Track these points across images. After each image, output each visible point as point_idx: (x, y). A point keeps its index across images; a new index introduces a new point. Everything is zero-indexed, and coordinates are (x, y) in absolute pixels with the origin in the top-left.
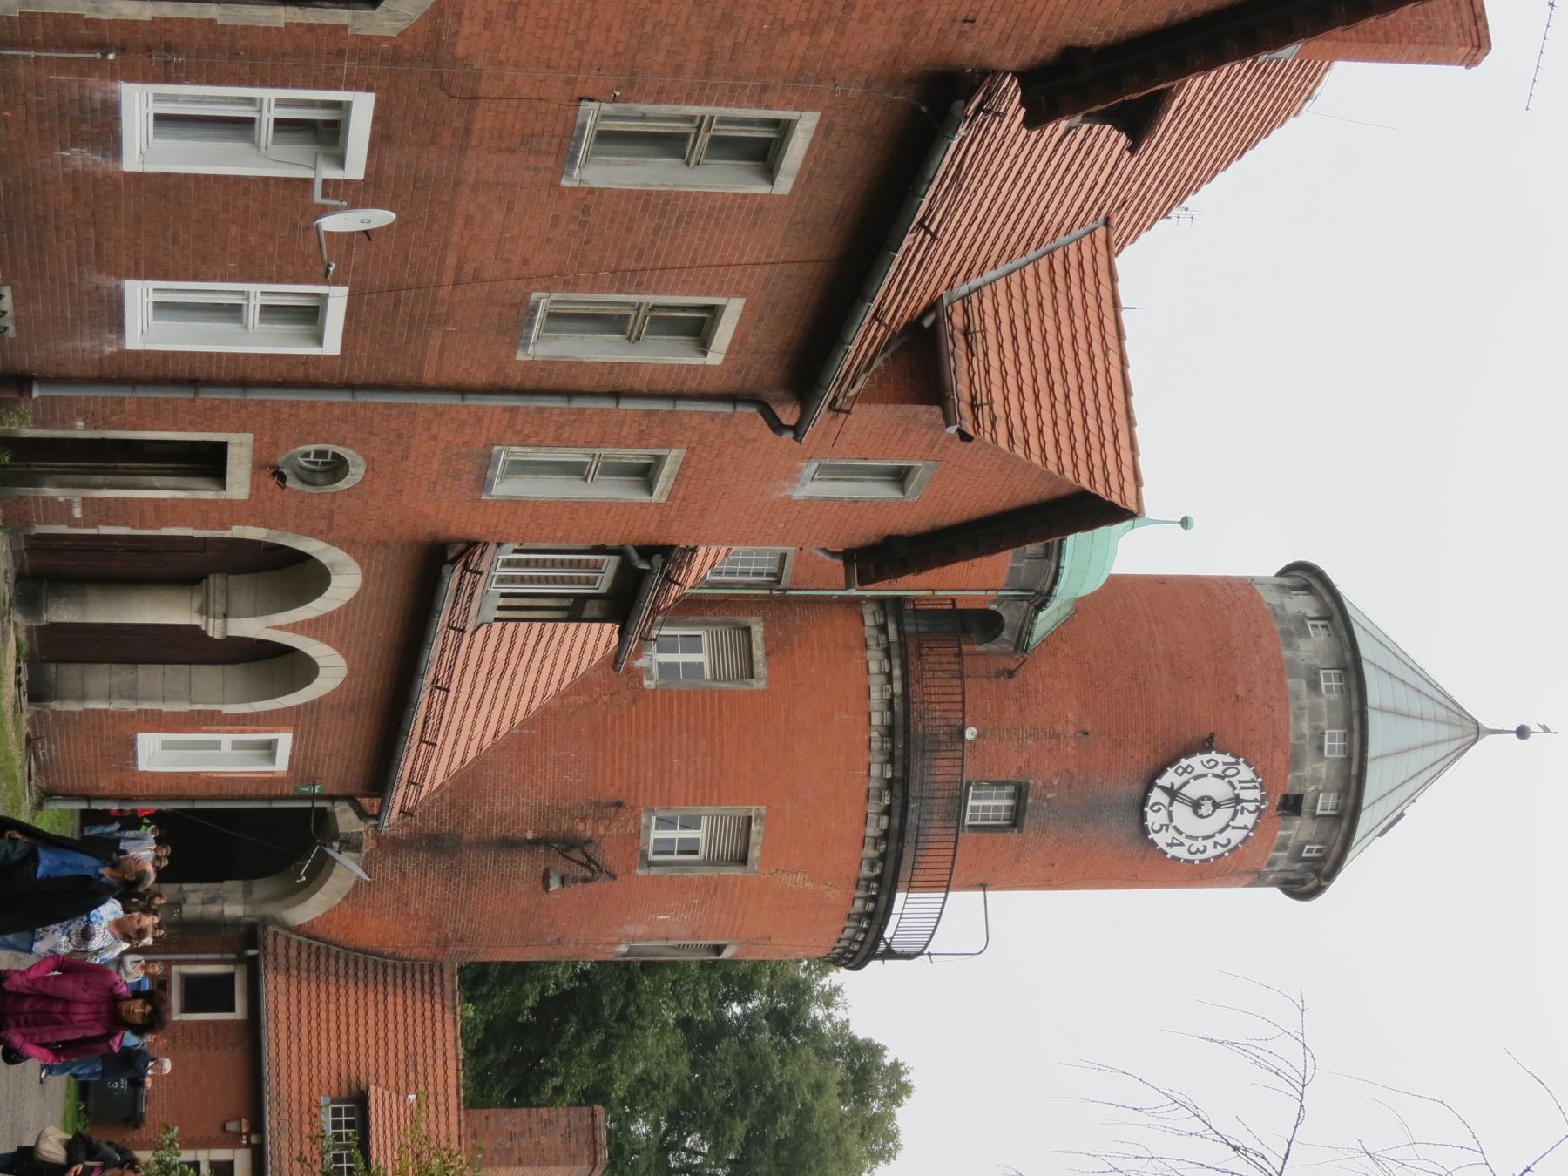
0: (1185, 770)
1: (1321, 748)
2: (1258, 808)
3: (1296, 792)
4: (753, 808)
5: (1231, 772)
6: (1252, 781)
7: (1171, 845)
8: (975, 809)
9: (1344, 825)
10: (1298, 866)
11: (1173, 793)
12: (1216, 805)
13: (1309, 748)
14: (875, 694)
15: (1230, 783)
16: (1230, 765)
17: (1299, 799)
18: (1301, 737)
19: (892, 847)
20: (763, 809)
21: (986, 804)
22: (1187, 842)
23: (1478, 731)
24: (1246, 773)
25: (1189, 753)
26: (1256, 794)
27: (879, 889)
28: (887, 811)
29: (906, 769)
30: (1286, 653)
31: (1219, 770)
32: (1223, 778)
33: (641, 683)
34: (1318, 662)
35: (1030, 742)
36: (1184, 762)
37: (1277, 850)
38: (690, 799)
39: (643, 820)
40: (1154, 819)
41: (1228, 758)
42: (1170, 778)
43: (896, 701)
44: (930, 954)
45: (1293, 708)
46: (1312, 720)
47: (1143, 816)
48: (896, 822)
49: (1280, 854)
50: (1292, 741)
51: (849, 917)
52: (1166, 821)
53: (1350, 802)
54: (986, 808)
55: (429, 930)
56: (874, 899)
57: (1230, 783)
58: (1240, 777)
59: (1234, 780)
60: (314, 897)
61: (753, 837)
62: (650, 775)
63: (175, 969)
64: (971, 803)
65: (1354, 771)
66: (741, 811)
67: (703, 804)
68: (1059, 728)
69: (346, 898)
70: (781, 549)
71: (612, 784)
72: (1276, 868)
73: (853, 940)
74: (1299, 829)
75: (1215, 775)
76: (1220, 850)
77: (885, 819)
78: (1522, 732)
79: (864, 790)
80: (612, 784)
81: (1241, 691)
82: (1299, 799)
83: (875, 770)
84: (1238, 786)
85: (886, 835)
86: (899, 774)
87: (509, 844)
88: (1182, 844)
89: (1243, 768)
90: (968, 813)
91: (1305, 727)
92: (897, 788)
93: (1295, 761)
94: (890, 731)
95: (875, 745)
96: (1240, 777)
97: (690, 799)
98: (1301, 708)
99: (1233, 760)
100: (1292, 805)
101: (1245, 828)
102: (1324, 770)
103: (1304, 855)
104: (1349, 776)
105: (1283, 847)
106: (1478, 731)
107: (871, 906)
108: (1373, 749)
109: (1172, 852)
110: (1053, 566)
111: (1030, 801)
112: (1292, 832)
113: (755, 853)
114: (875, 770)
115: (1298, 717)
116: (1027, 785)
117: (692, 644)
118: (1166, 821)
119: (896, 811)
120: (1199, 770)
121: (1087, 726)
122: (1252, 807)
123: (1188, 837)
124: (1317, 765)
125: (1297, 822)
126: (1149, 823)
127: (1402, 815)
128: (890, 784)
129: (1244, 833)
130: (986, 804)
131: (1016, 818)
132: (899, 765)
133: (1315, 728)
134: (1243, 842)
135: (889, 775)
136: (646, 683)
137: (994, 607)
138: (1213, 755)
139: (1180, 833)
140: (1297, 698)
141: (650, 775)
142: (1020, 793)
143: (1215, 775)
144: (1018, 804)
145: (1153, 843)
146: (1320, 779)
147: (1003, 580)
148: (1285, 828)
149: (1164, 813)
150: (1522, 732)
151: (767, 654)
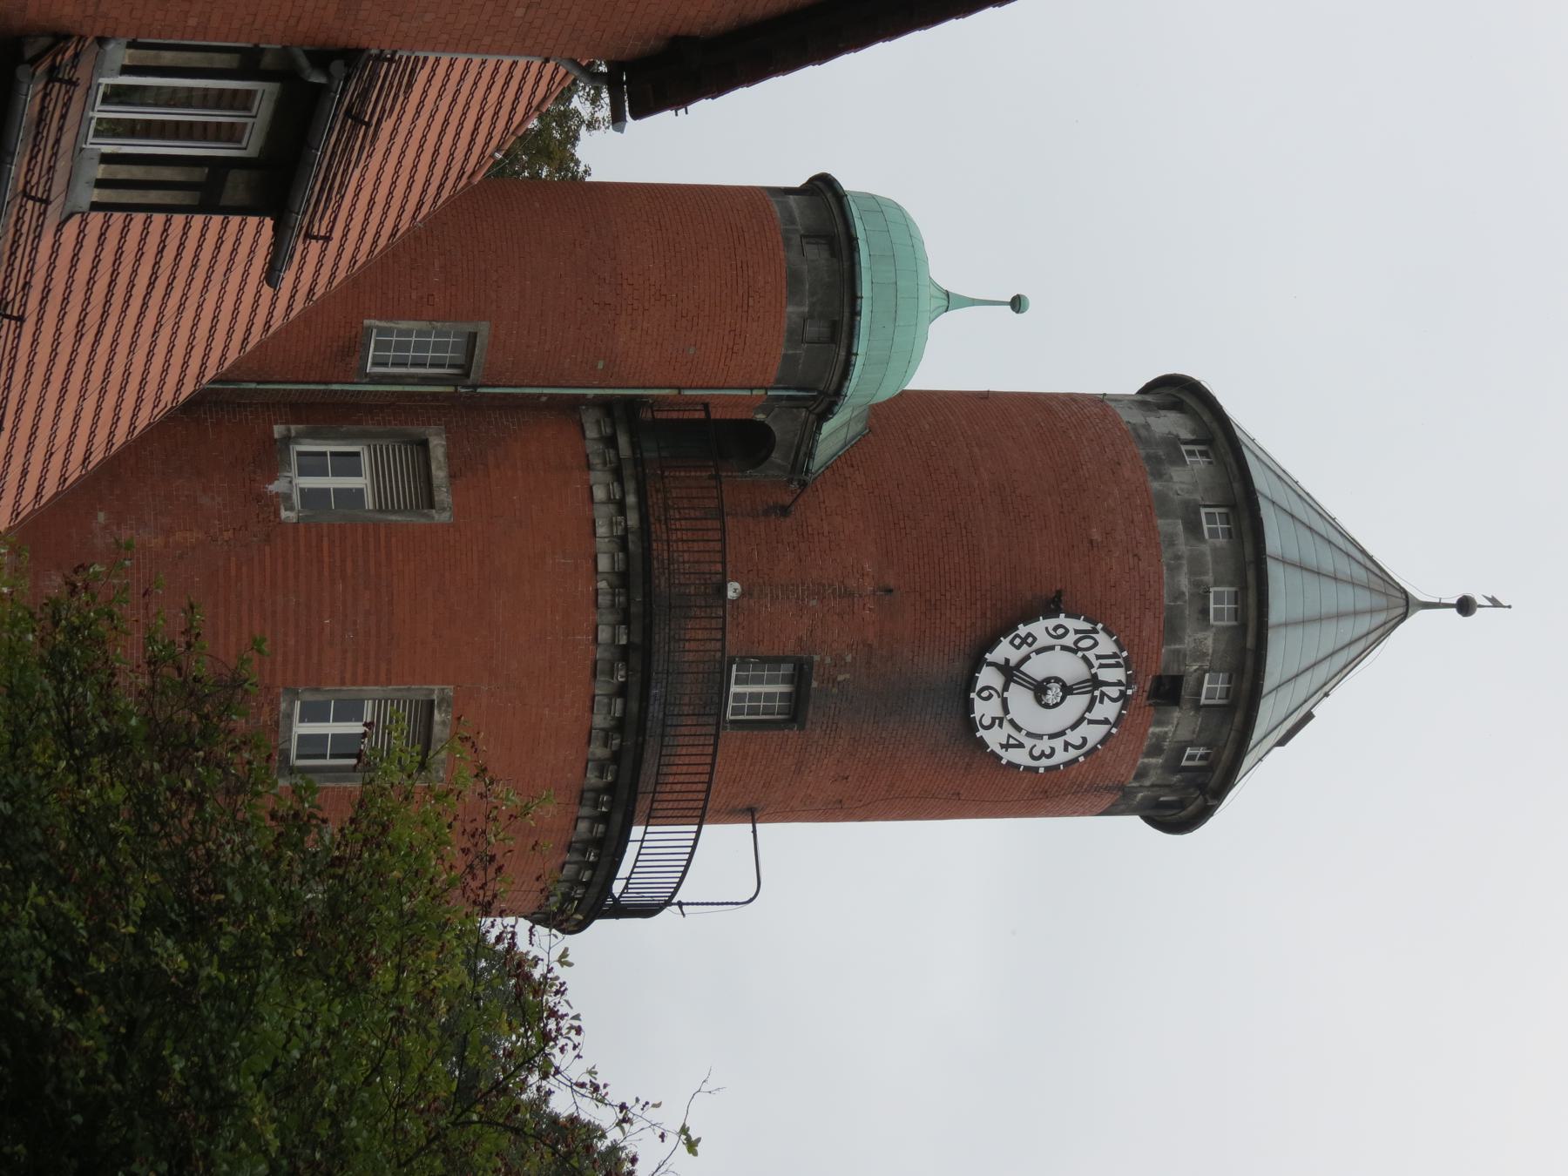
0: (1024, 641)
1: (1205, 612)
2: (1123, 694)
3: (1174, 671)
4: (436, 688)
6: (1114, 656)
7: (1006, 746)
8: (739, 697)
9: (1238, 718)
10: (1176, 778)
11: (1010, 672)
12: (1067, 690)
13: (1189, 611)
14: (602, 530)
15: (1085, 658)
16: (1085, 634)
19: (629, 743)
20: (450, 690)
21: (756, 691)
22: (1028, 742)
23: (1407, 605)
24: (1106, 645)
25: (1029, 618)
26: (1118, 674)
27: (612, 804)
28: (622, 691)
29: (648, 632)
30: (1155, 485)
31: (1069, 640)
32: (1074, 650)
33: (277, 514)
34: (1198, 497)
35: (814, 603)
36: (1022, 630)
37: (1148, 754)
38: (348, 676)
39: (283, 706)
40: (984, 710)
42: (1004, 651)
43: (630, 537)
44: (680, 904)
45: (1166, 556)
46: (1192, 573)
47: (969, 706)
48: (634, 706)
49: (1153, 761)
50: (1166, 601)
51: (569, 847)
52: (1000, 714)
53: (1246, 685)
54: (755, 697)
56: (605, 818)
57: (1085, 658)
58: (1098, 650)
59: (1090, 655)
61: (437, 729)
62: (292, 642)
64: (734, 689)
65: (1250, 642)
66: (418, 692)
67: (365, 683)
68: (852, 583)
70: (468, 327)
72: (1147, 783)
73: (575, 882)
74: (1178, 725)
75: (1064, 648)
76: (1072, 753)
77: (619, 702)
78: (1465, 606)
79: (589, 663)
81: (1096, 535)
83: (604, 634)
84: (1096, 663)
85: (620, 726)
86: (637, 639)
88: (1021, 745)
89: (1101, 637)
90: (731, 703)
91: (1184, 583)
93: (1172, 630)
94: (622, 579)
95: (604, 600)
96: (1098, 650)
97: (348, 676)
98: (1178, 557)
99: (1088, 626)
100: (1168, 691)
101: (1106, 721)
102: (1210, 642)
103: (1184, 763)
104: (1244, 649)
105: (1155, 750)
106: (1407, 605)
107: (601, 828)
108: (1276, 613)
110: (843, 353)
111: (814, 684)
112: (1169, 729)
114: (604, 634)
115: (1174, 570)
116: (811, 662)
117: (347, 464)
118: (1000, 714)
119: (634, 691)
120: (1043, 640)
121: (891, 582)
122: (1114, 692)
123: (1029, 734)
124: (1200, 635)
125: (1176, 714)
126: (977, 715)
127: (1309, 717)
128: (624, 653)
129: (1104, 729)
130: (756, 691)
131: (796, 709)
133: (1196, 584)
134: (1103, 742)
135: (623, 641)
136: (284, 514)
137: (760, 417)
138: (1062, 619)
139: (1019, 729)
140: (1172, 544)
141: (292, 642)
142: (801, 675)
143: (1064, 648)
145: (982, 744)
146: (1205, 654)
147: (773, 373)
148: (1159, 723)
149: (996, 700)
150: (1465, 606)
151: (452, 476)
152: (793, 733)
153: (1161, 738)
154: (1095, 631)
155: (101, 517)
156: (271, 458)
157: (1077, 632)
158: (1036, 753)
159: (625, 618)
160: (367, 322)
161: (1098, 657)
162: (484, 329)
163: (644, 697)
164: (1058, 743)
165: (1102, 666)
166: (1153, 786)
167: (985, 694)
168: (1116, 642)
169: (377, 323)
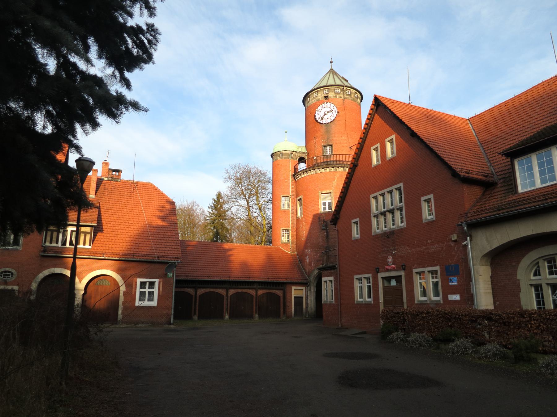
11: (322, 119)
13: (317, 98)
17: (325, 97)
24: (319, 108)
40: (329, 121)
74: (331, 95)
78: (331, 62)
82: (327, 96)
87: (327, 237)
93: (318, 100)
100: (326, 97)
105: (336, 96)
109: (335, 116)
113: (328, 191)
125: (329, 96)
127: (343, 78)
142: (325, 146)
150: (331, 62)
152: (333, 145)
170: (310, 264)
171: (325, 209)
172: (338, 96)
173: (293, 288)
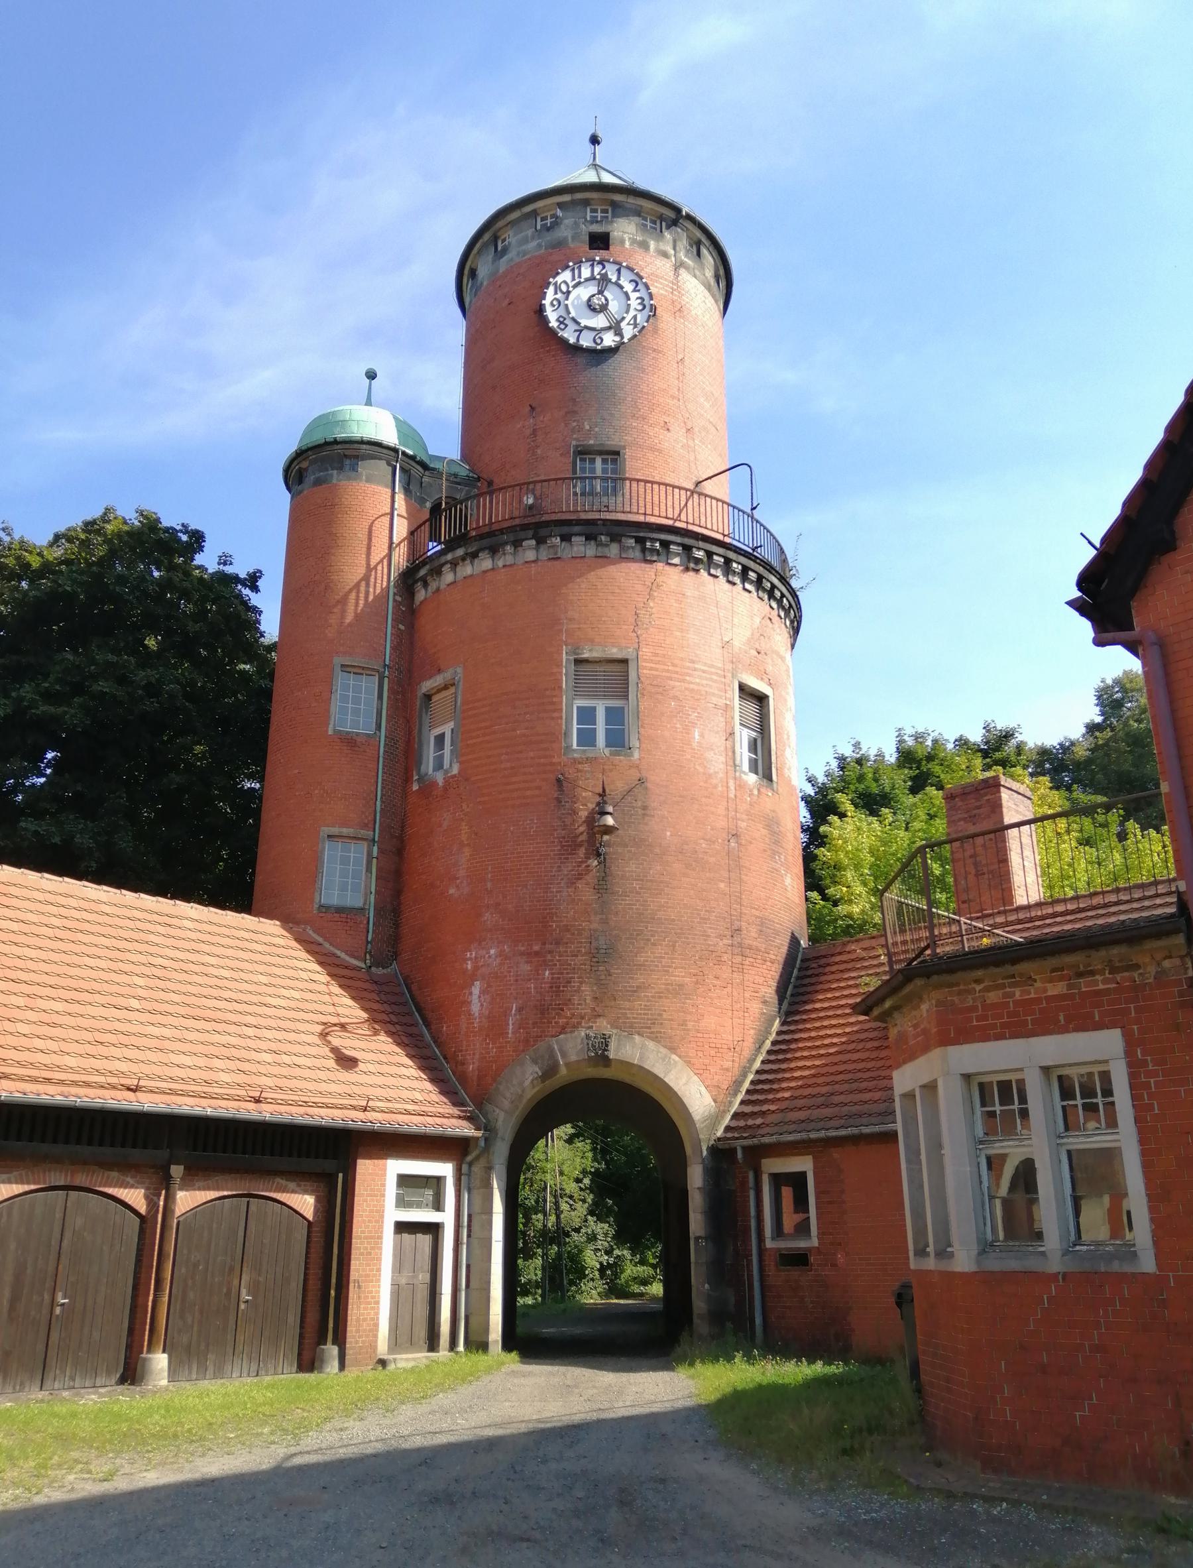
2: (599, 263)
5: (564, 288)
6: (573, 270)
15: (575, 286)
16: (557, 289)
18: (539, 245)
24: (566, 276)
27: (653, 540)
28: (566, 538)
29: (525, 527)
32: (568, 292)
33: (454, 776)
35: (539, 451)
41: (550, 292)
43: (470, 550)
45: (517, 260)
48: (577, 529)
55: (719, 962)
56: (665, 544)
58: (569, 280)
59: (571, 284)
60: (671, 1084)
62: (532, 754)
63: (769, 1244)
68: (528, 432)
69: (673, 1050)
70: (338, 669)
71: (539, 788)
72: (672, 252)
78: (595, 140)
79: (550, 563)
80: (539, 788)
83: (530, 555)
85: (589, 537)
86: (531, 533)
88: (635, 317)
89: (559, 279)
92: (543, 532)
94: (494, 551)
96: (569, 280)
98: (518, 255)
101: (619, 271)
110: (364, 446)
116: (577, 446)
119: (565, 530)
120: (562, 311)
122: (597, 269)
123: (627, 312)
125: (615, 235)
126: (613, 344)
128: (541, 541)
132: (522, 535)
133: (533, 238)
135: (533, 542)
137: (428, 505)
138: (547, 302)
140: (512, 260)
141: (532, 754)
144: (600, 453)
146: (575, 223)
148: (622, 242)
151: (439, 671)
153: (633, 241)
154: (556, 284)
155: (451, 891)
156: (428, 787)
157: (556, 293)
158: (640, 307)
159: (517, 544)
160: (330, 732)
161: (574, 279)
162: (338, 661)
163: (568, 523)
164: (633, 296)
165: (580, 277)
166: (674, 249)
167: (599, 341)
168: (563, 270)
169: (331, 726)
170: (495, 1026)
171: (587, 738)
172: (652, 245)
173: (397, 1167)
